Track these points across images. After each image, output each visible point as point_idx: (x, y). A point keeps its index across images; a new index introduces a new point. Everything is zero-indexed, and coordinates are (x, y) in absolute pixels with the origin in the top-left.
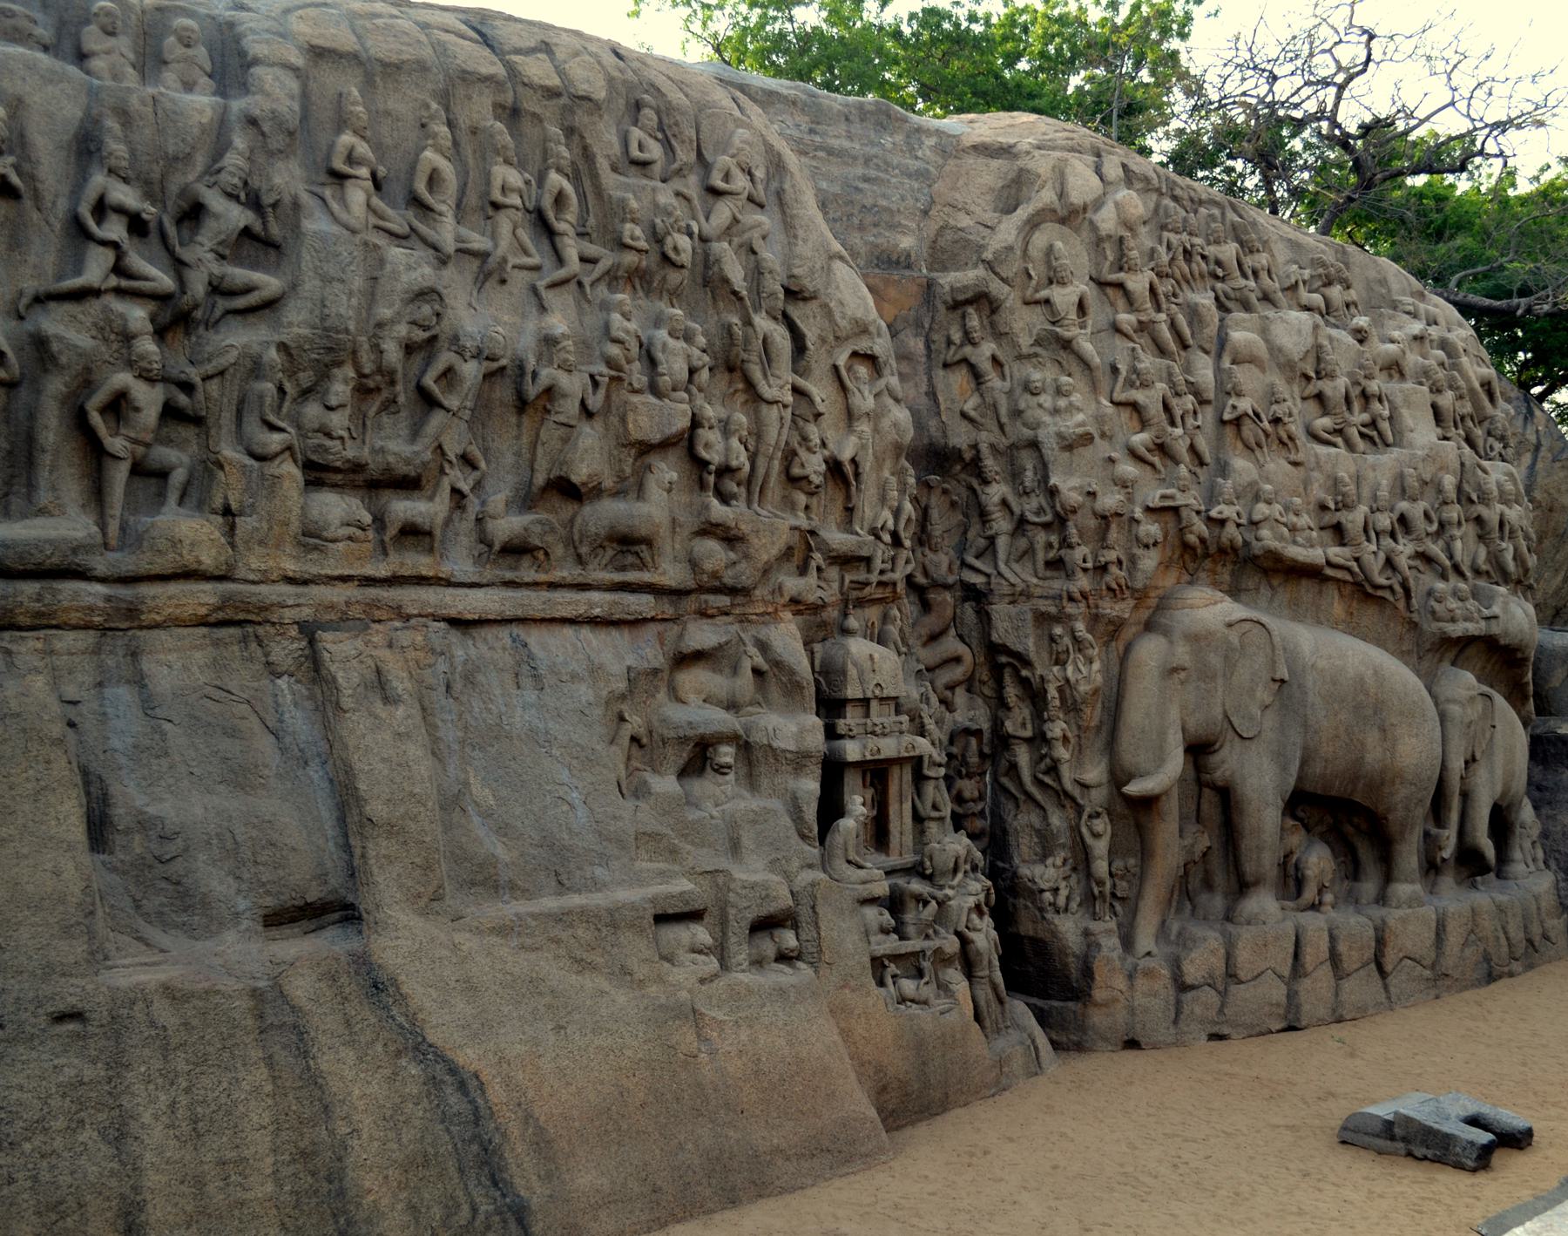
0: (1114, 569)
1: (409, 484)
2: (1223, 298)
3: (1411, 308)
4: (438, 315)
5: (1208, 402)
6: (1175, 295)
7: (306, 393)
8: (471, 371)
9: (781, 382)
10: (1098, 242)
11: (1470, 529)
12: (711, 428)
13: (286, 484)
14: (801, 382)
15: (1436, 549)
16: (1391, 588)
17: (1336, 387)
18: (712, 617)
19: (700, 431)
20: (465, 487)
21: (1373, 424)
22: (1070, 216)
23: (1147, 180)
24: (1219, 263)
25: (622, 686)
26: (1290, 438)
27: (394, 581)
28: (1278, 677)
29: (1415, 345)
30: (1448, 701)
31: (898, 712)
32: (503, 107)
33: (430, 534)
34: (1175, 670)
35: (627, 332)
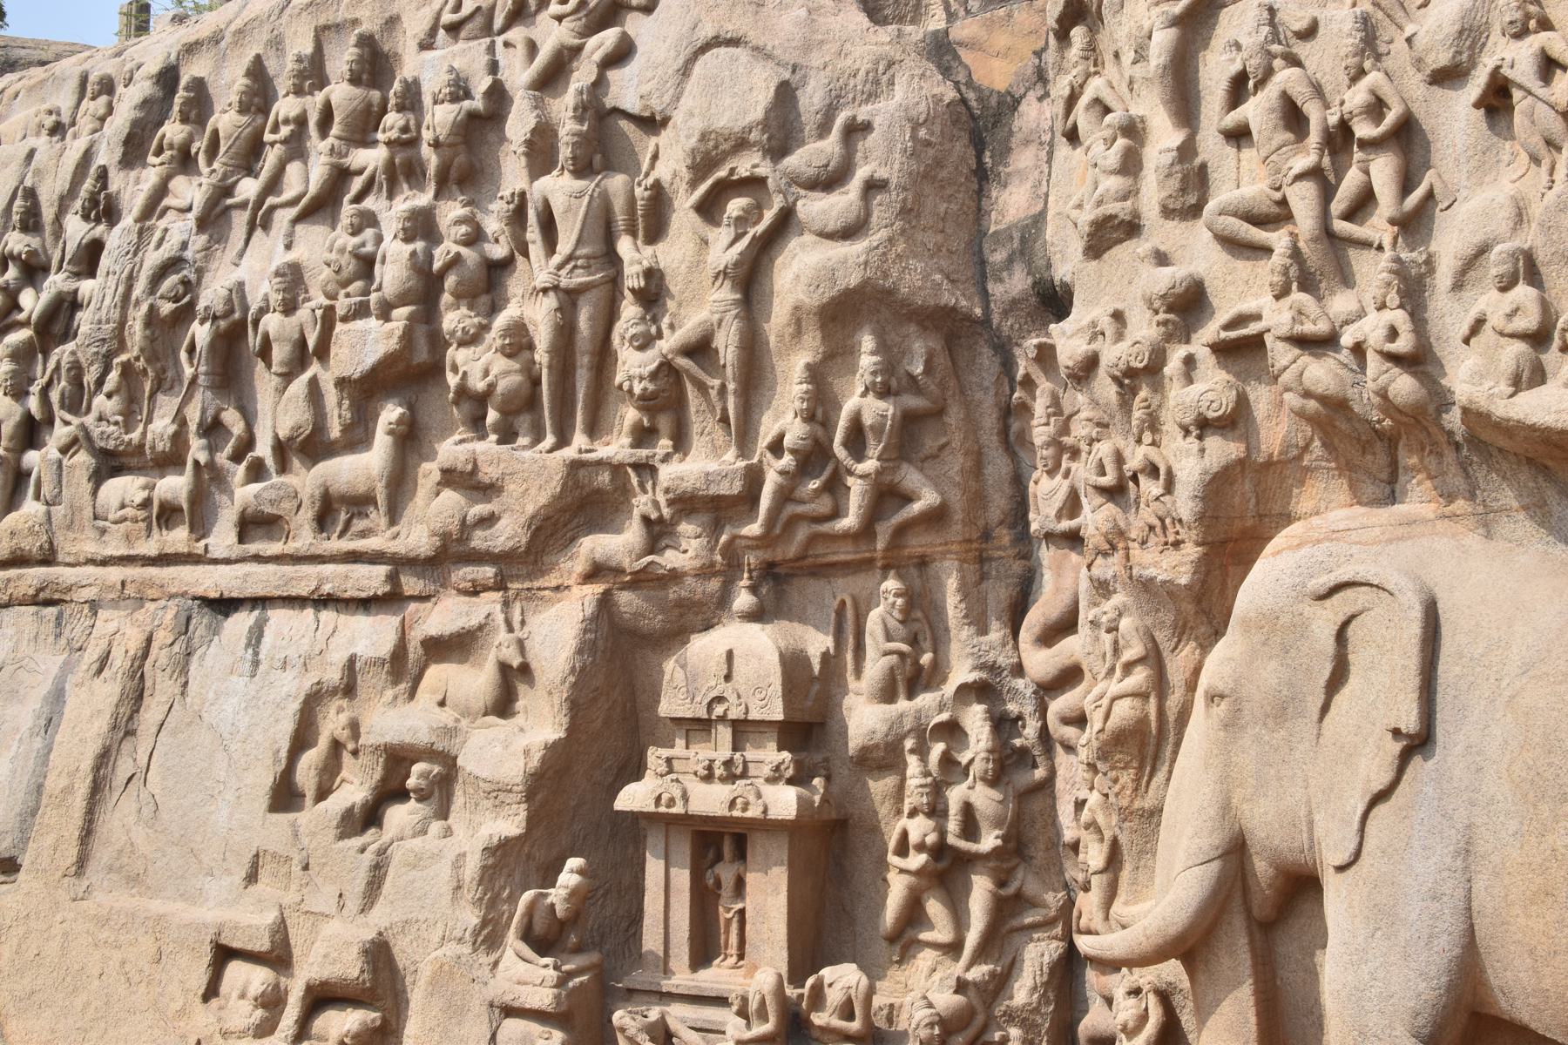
1: (171, 460)
4: (186, 283)
7: (100, 382)
8: (201, 333)
9: (557, 259)
12: (462, 344)
13: (77, 472)
14: (624, 246)
18: (475, 593)
19: (450, 351)
20: (203, 458)
25: (334, 676)
27: (164, 560)
31: (779, 750)
32: (326, 28)
33: (181, 510)
34: (1213, 697)
35: (342, 251)
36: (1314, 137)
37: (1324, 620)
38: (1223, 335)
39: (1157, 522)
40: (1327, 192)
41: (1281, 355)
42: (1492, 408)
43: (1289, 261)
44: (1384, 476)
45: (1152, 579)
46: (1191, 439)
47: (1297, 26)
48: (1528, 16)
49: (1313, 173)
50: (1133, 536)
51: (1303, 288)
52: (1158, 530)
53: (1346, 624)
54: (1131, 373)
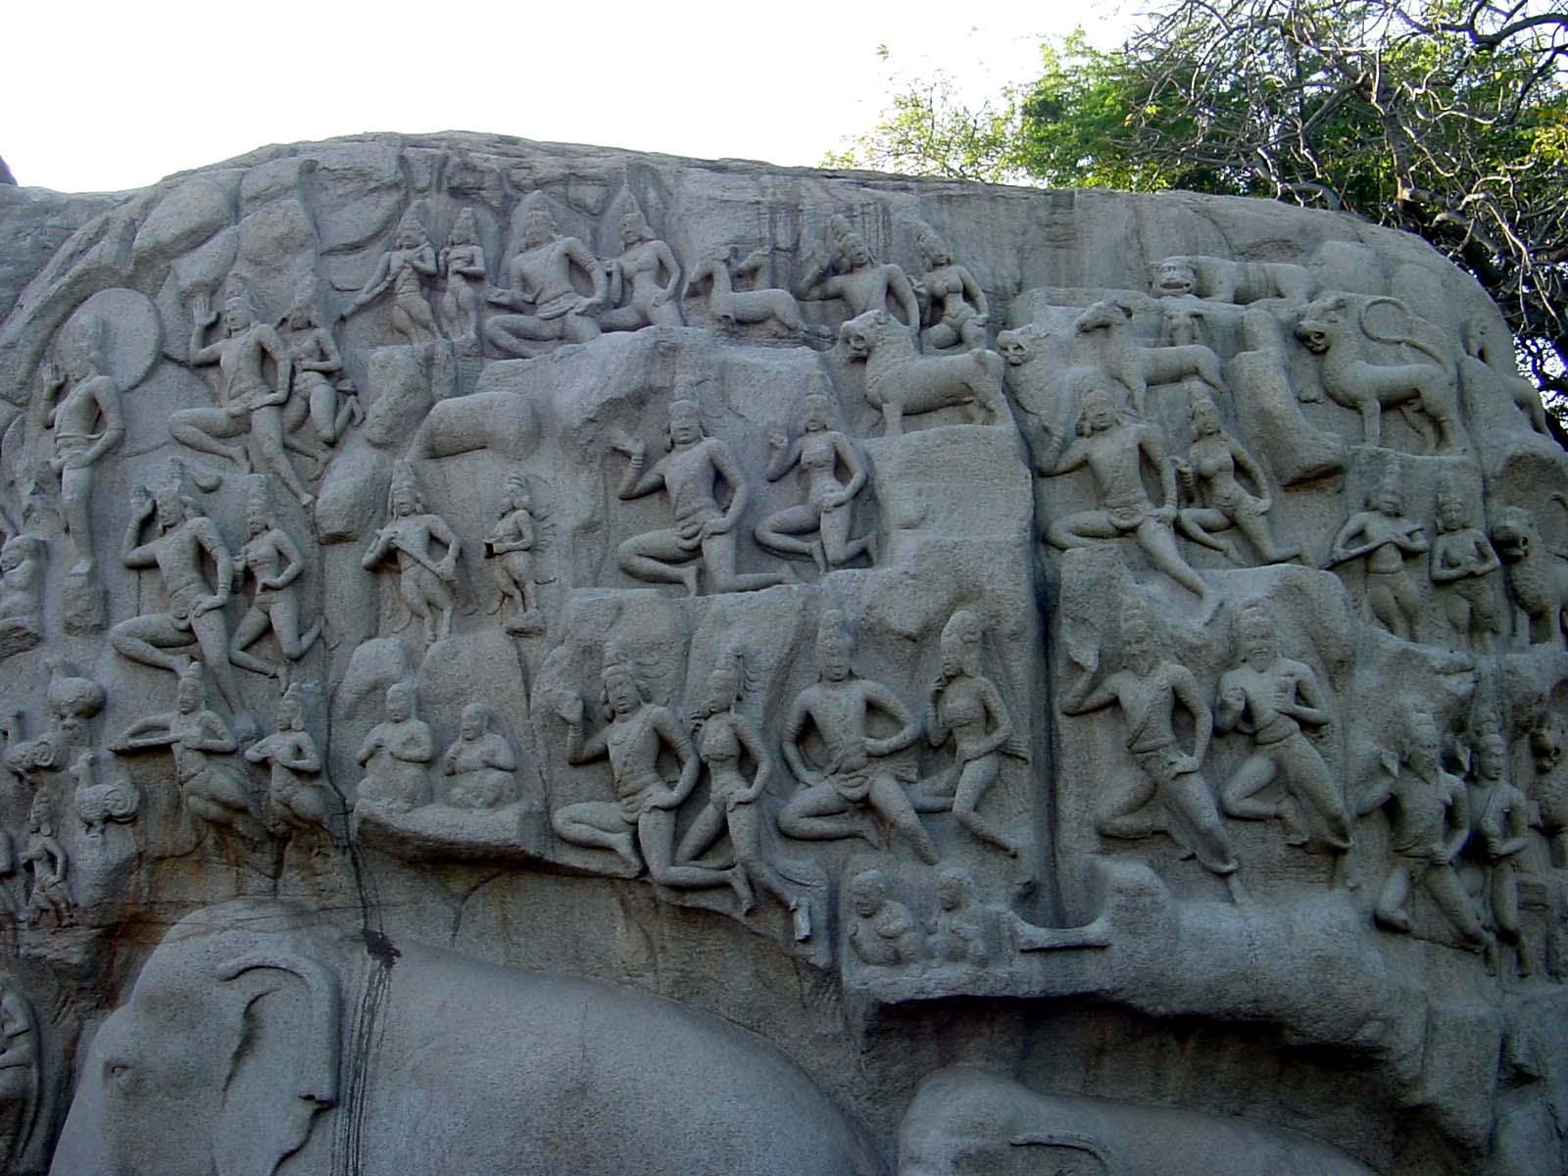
0: (40, 869)
2: (508, 340)
3: (1177, 276)
5: (338, 538)
6: (324, 356)
10: (185, 299)
11: (1102, 735)
15: (886, 790)
16: (724, 886)
17: (681, 468)
21: (812, 530)
22: (145, 269)
23: (362, 175)
24: (525, 283)
26: (516, 583)
28: (305, 1088)
29: (1086, 344)
30: (915, 1160)
34: (112, 1068)
36: (223, 579)
37: (231, 1001)
38: (132, 742)
39: (52, 908)
40: (231, 632)
41: (191, 763)
42: (391, 821)
43: (198, 683)
44: (270, 872)
45: (39, 958)
46: (94, 832)
47: (204, 483)
48: (417, 500)
49: (221, 607)
50: (21, 918)
51: (208, 708)
52: (51, 913)
53: (252, 1002)
54: (35, 769)
